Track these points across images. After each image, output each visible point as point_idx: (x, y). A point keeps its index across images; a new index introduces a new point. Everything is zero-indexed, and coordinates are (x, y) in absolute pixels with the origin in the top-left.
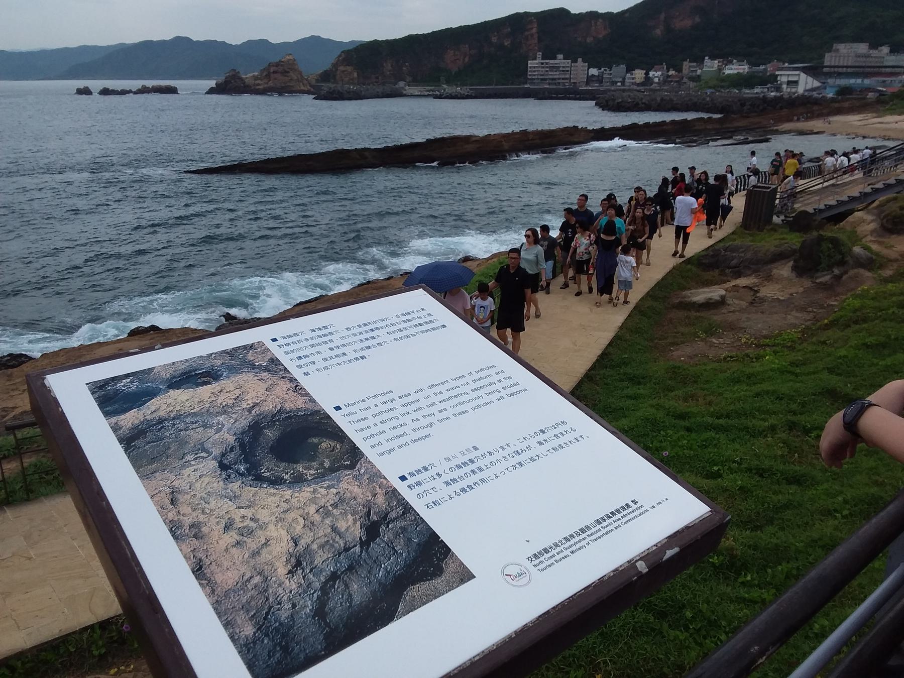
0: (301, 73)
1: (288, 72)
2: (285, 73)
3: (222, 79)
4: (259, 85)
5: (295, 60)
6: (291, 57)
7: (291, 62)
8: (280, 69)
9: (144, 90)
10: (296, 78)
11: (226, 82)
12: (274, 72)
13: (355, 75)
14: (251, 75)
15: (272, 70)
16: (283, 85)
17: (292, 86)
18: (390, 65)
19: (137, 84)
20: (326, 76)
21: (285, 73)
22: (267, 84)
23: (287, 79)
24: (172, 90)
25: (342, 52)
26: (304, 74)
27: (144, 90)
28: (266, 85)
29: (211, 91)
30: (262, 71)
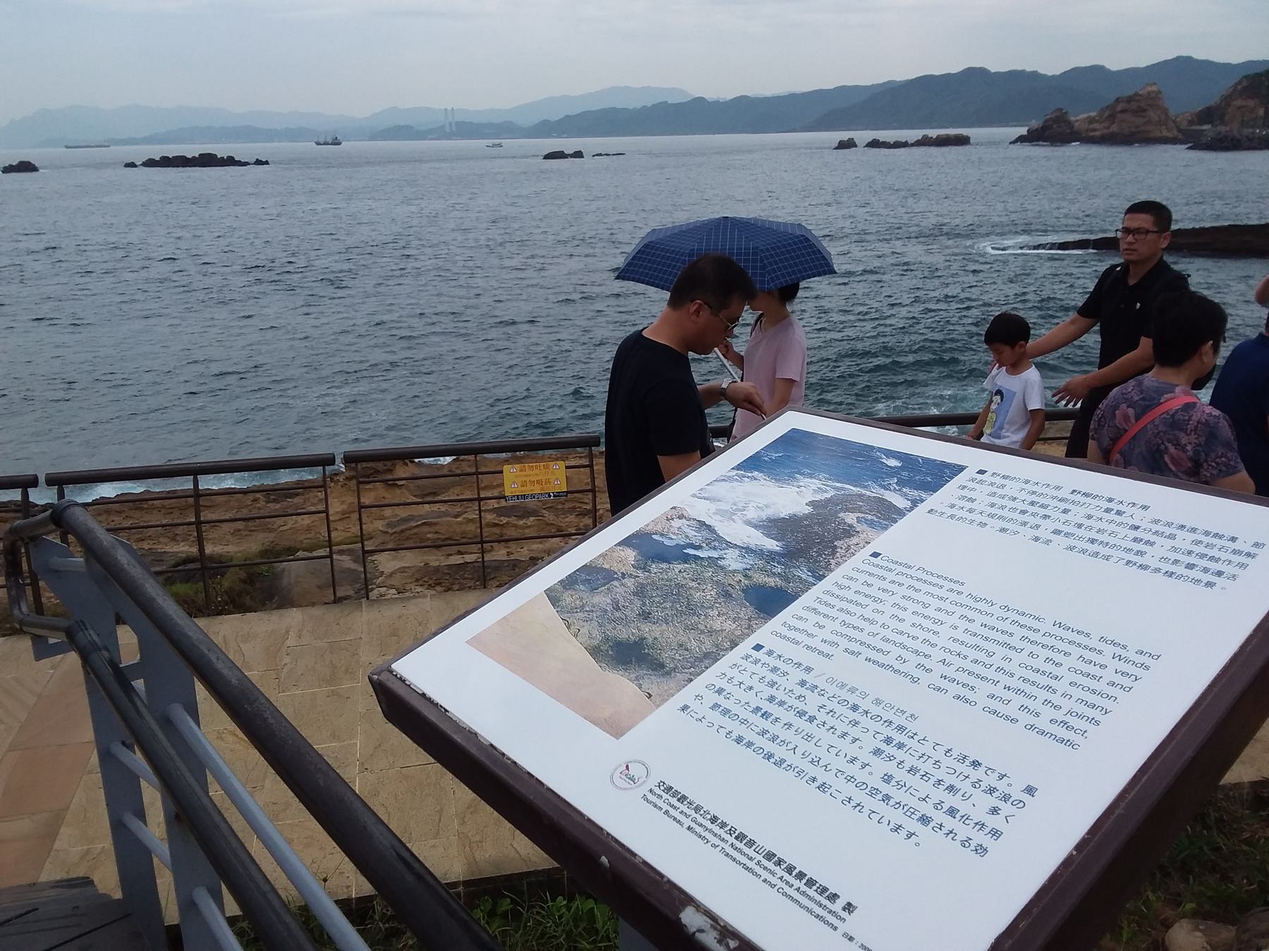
0: (1165, 112)
1: (1145, 111)
2: (1140, 111)
3: (1036, 123)
4: (1094, 130)
5: (1160, 92)
6: (1154, 88)
7: (1153, 95)
8: (1134, 105)
9: (925, 142)
10: (1157, 118)
11: (1044, 128)
12: (1123, 111)
13: (1261, 112)
15: (1119, 108)
16: (1133, 130)
17: (1149, 131)
20: (1208, 115)
21: (1140, 111)
22: (1108, 128)
25: (1244, 77)
26: (1172, 112)
27: (925, 142)
28: (1106, 131)
30: (1103, 111)
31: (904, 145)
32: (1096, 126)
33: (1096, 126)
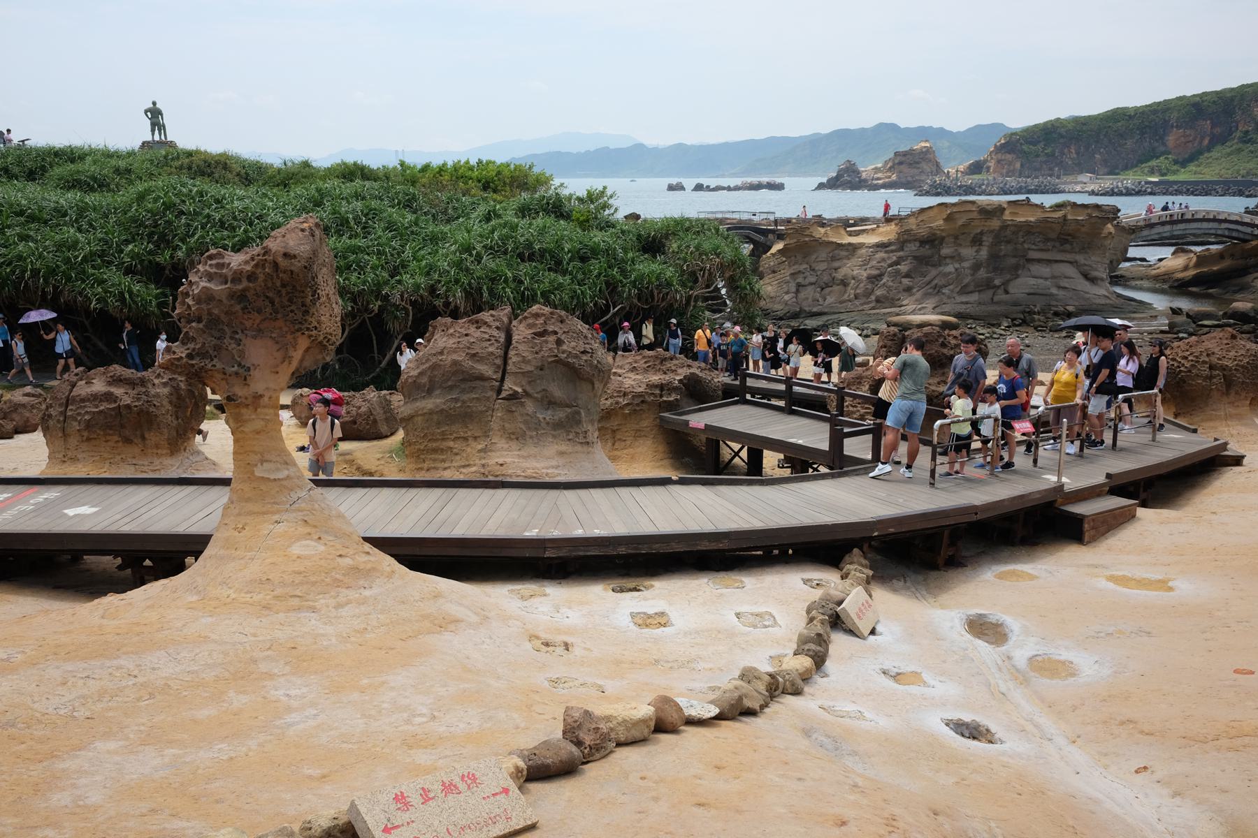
1: (918, 163)
4: (878, 179)
11: (837, 178)
13: (1018, 165)
14: (873, 167)
16: (910, 179)
18: (1073, 151)
19: (738, 181)
23: (916, 171)
24: (780, 187)
28: (887, 180)
29: (821, 186)
31: (718, 188)
32: (879, 175)
33: (879, 175)
